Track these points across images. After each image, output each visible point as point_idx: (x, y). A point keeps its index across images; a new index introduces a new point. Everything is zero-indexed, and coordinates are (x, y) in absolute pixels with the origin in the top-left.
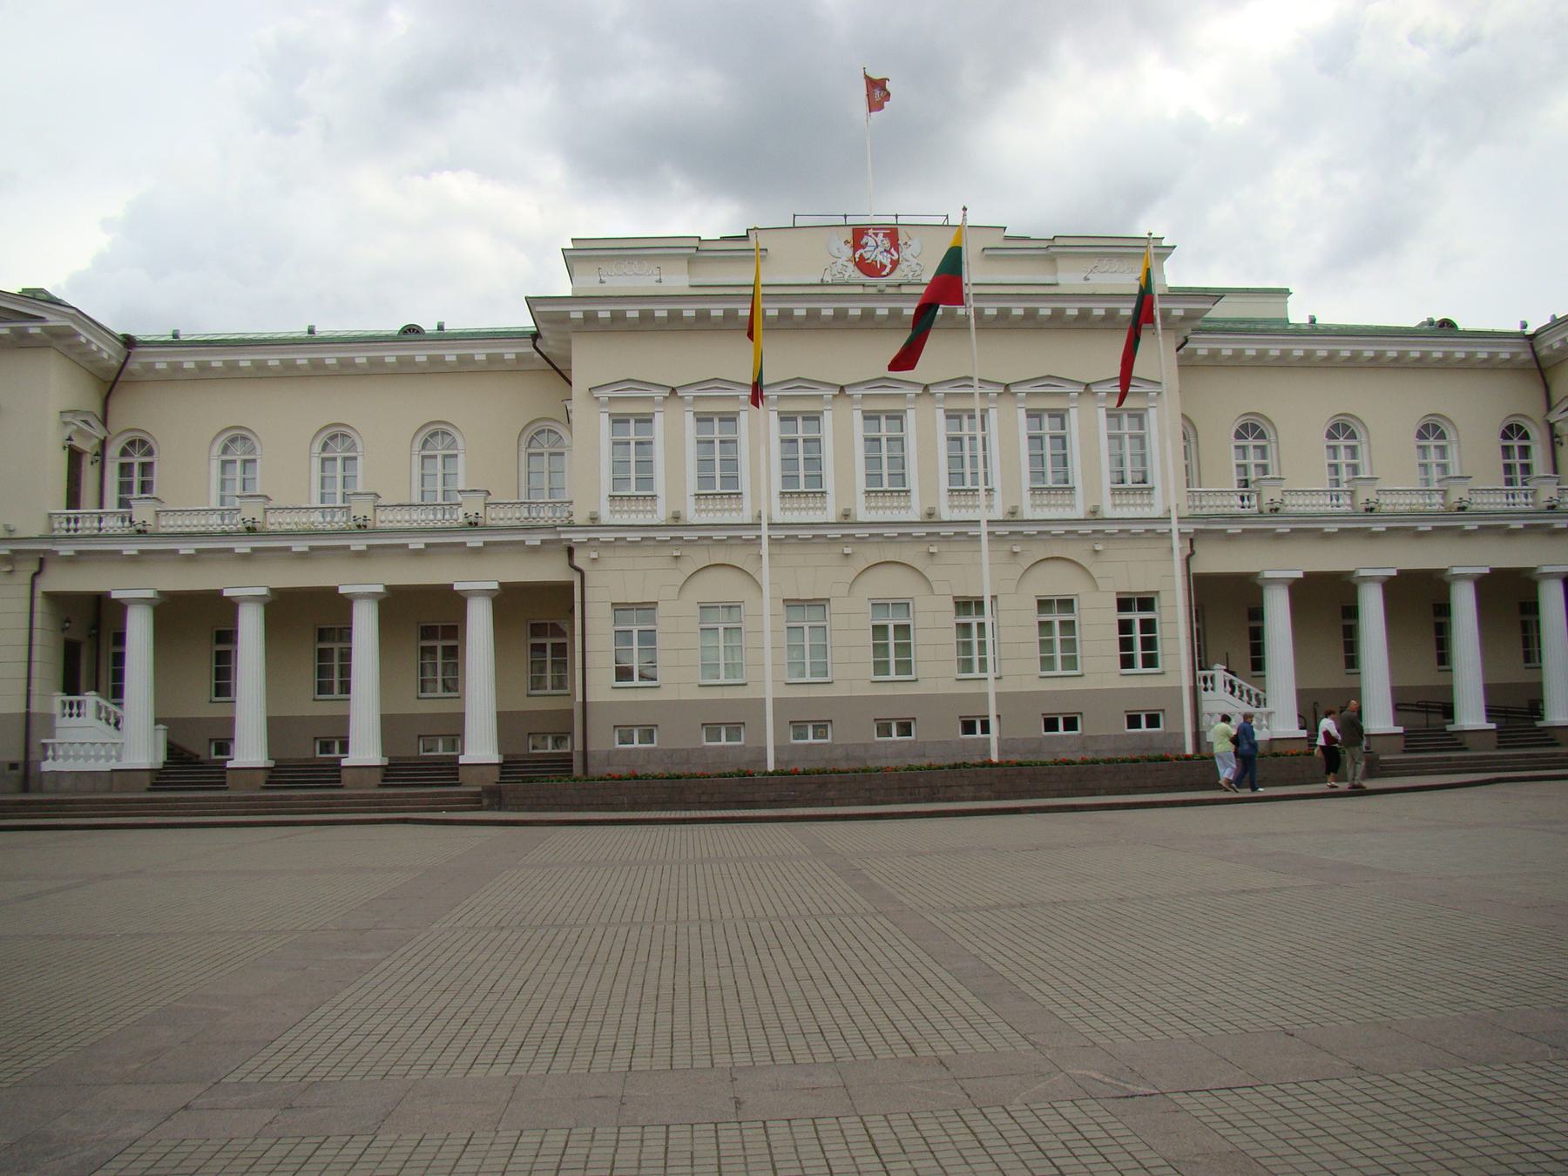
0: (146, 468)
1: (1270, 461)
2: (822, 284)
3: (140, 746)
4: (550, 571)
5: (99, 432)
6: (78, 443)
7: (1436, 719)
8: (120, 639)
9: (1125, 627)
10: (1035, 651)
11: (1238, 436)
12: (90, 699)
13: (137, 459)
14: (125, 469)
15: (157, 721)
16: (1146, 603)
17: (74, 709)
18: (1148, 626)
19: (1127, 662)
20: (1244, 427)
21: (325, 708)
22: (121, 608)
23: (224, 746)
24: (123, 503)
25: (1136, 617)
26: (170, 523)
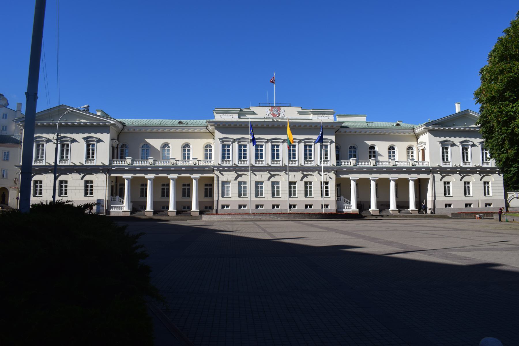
1: (357, 154)
2: (265, 119)
5: (117, 143)
11: (350, 148)
14: (122, 150)
15: (131, 202)
20: (351, 147)
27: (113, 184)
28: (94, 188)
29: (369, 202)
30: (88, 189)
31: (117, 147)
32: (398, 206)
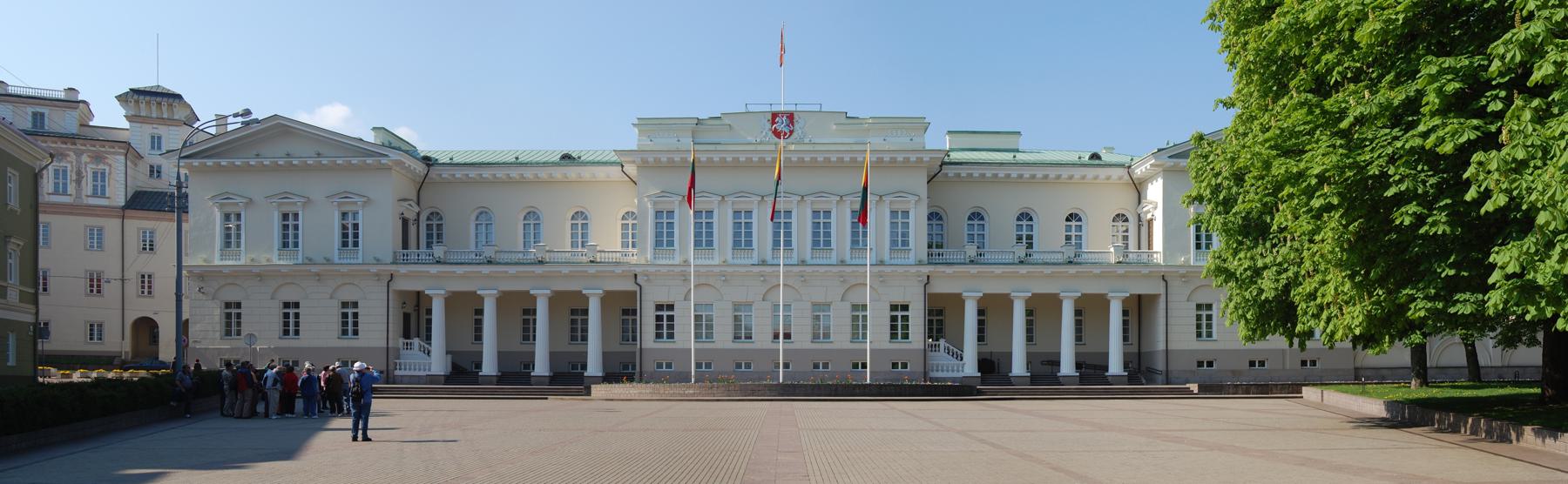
0: (439, 226)
3: (438, 364)
4: (629, 286)
5: (417, 209)
6: (406, 215)
7: (1048, 369)
8: (429, 312)
9: (894, 319)
10: (849, 329)
12: (416, 341)
13: (435, 222)
14: (429, 227)
16: (905, 308)
17: (408, 346)
18: (905, 318)
19: (893, 336)
21: (525, 348)
22: (430, 299)
23: (479, 366)
24: (429, 245)
25: (899, 314)
26: (453, 258)
27: (410, 309)
28: (360, 319)
29: (1010, 355)
30: (349, 322)
31: (417, 220)
32: (1078, 366)
